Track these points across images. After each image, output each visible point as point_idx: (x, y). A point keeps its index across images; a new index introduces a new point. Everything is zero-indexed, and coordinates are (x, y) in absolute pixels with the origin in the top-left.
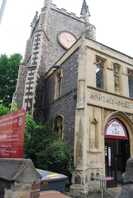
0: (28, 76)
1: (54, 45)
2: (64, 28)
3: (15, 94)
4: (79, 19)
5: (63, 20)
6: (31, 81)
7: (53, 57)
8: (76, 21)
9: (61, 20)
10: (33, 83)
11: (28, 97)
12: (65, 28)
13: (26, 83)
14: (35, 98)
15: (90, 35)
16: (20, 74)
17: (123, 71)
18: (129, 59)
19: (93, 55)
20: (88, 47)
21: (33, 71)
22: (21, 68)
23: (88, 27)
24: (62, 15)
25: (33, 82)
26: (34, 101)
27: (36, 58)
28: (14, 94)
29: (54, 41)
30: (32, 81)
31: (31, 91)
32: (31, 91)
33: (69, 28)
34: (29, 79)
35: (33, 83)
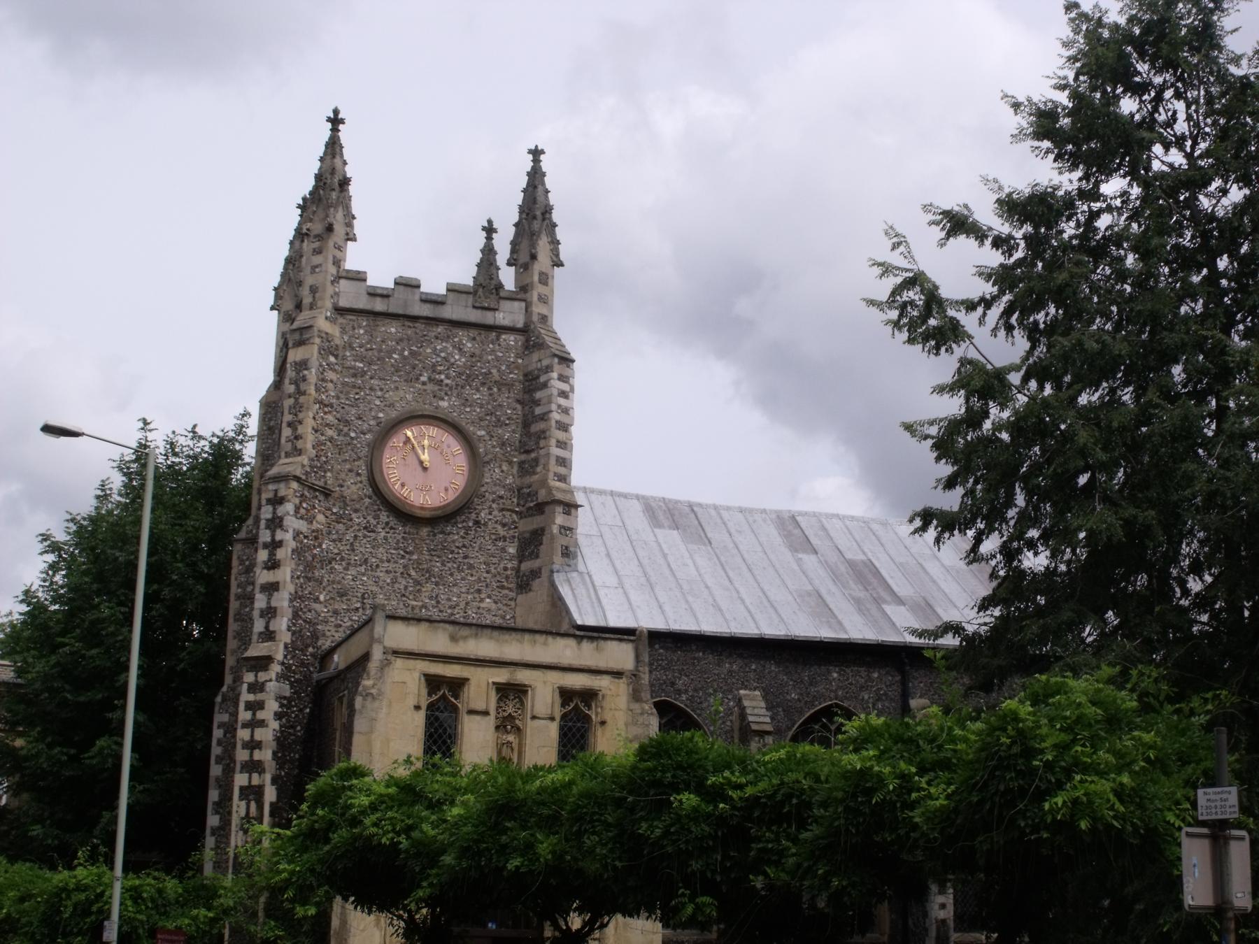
0: (246, 696)
1: (356, 511)
2: (405, 398)
3: (224, 700)
4: (488, 318)
5: (401, 354)
6: (254, 714)
7: (352, 571)
8: (473, 333)
9: (390, 353)
10: (262, 724)
11: (250, 778)
12: (409, 397)
13: (240, 724)
14: (274, 781)
15: (538, 411)
16: (238, 597)
17: (533, 706)
18: (579, 643)
19: (416, 675)
20: (396, 653)
21: (262, 676)
22: (242, 562)
23: (535, 356)
24: (393, 328)
25: (263, 721)
26: (270, 794)
27: (270, 613)
28: (219, 699)
29: (354, 487)
30: (261, 715)
31: (257, 755)
32: (257, 755)
33: (430, 387)
34: (250, 706)
35: (262, 724)
